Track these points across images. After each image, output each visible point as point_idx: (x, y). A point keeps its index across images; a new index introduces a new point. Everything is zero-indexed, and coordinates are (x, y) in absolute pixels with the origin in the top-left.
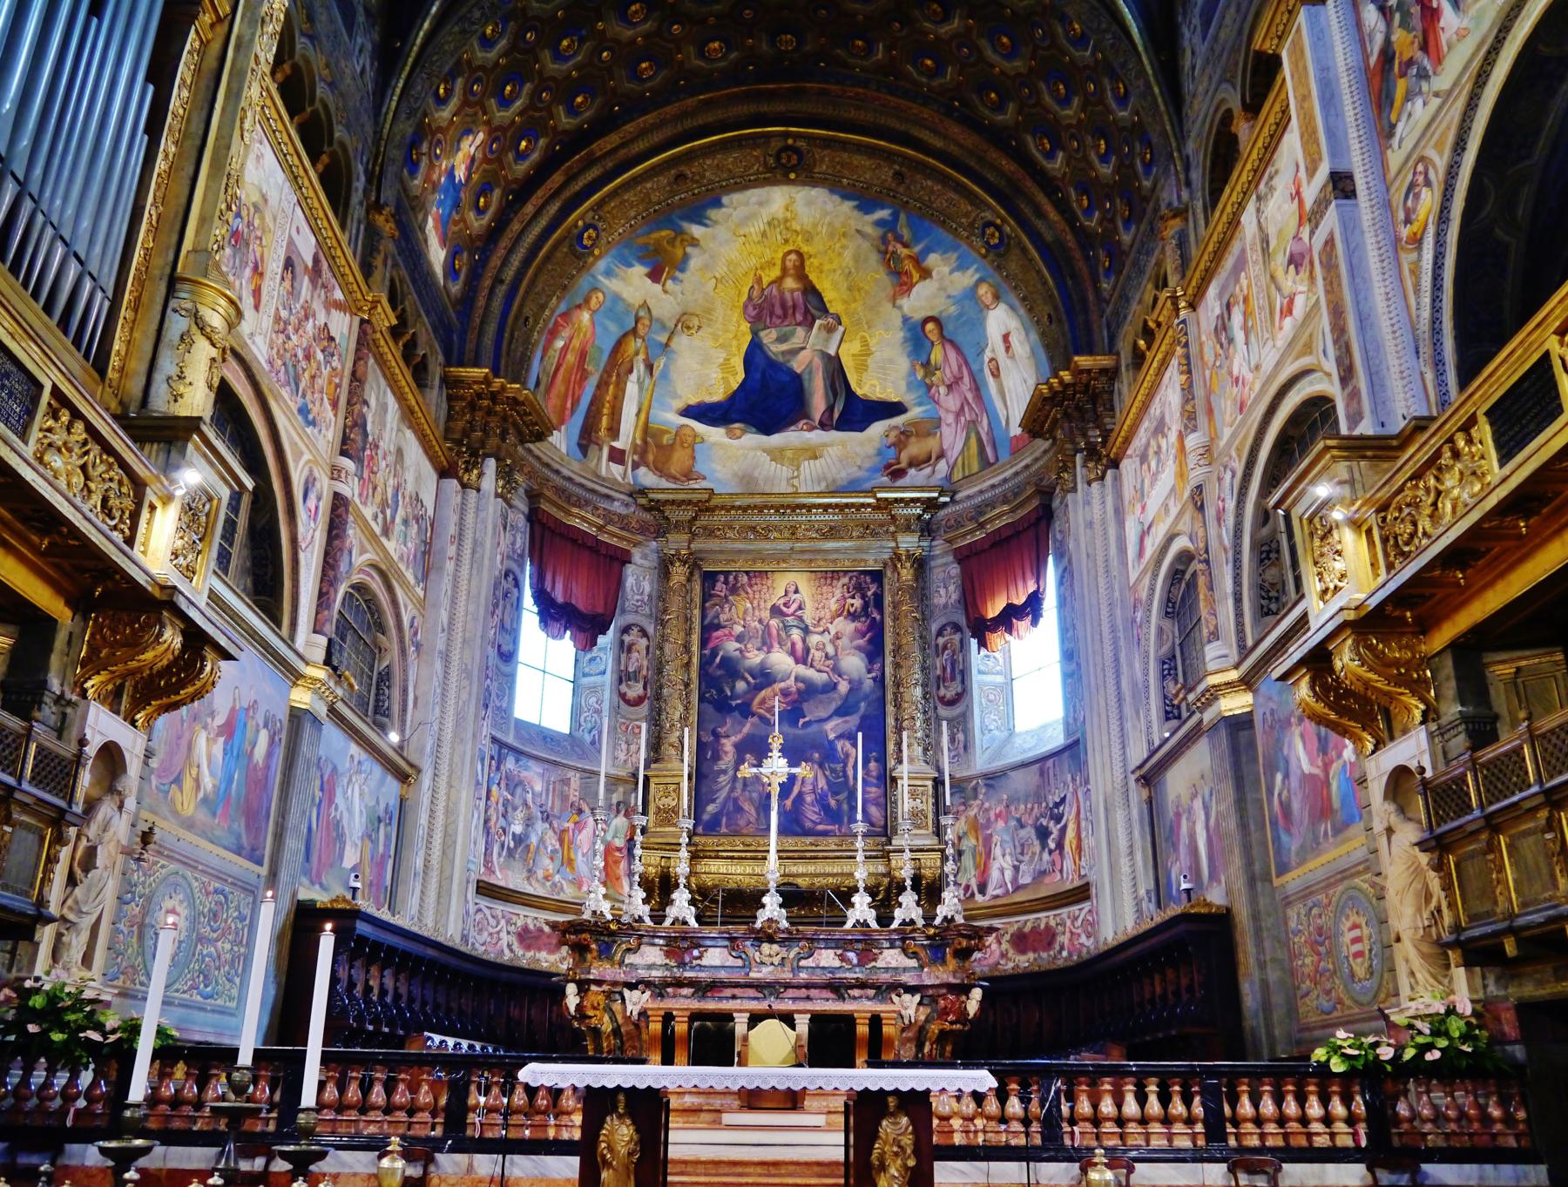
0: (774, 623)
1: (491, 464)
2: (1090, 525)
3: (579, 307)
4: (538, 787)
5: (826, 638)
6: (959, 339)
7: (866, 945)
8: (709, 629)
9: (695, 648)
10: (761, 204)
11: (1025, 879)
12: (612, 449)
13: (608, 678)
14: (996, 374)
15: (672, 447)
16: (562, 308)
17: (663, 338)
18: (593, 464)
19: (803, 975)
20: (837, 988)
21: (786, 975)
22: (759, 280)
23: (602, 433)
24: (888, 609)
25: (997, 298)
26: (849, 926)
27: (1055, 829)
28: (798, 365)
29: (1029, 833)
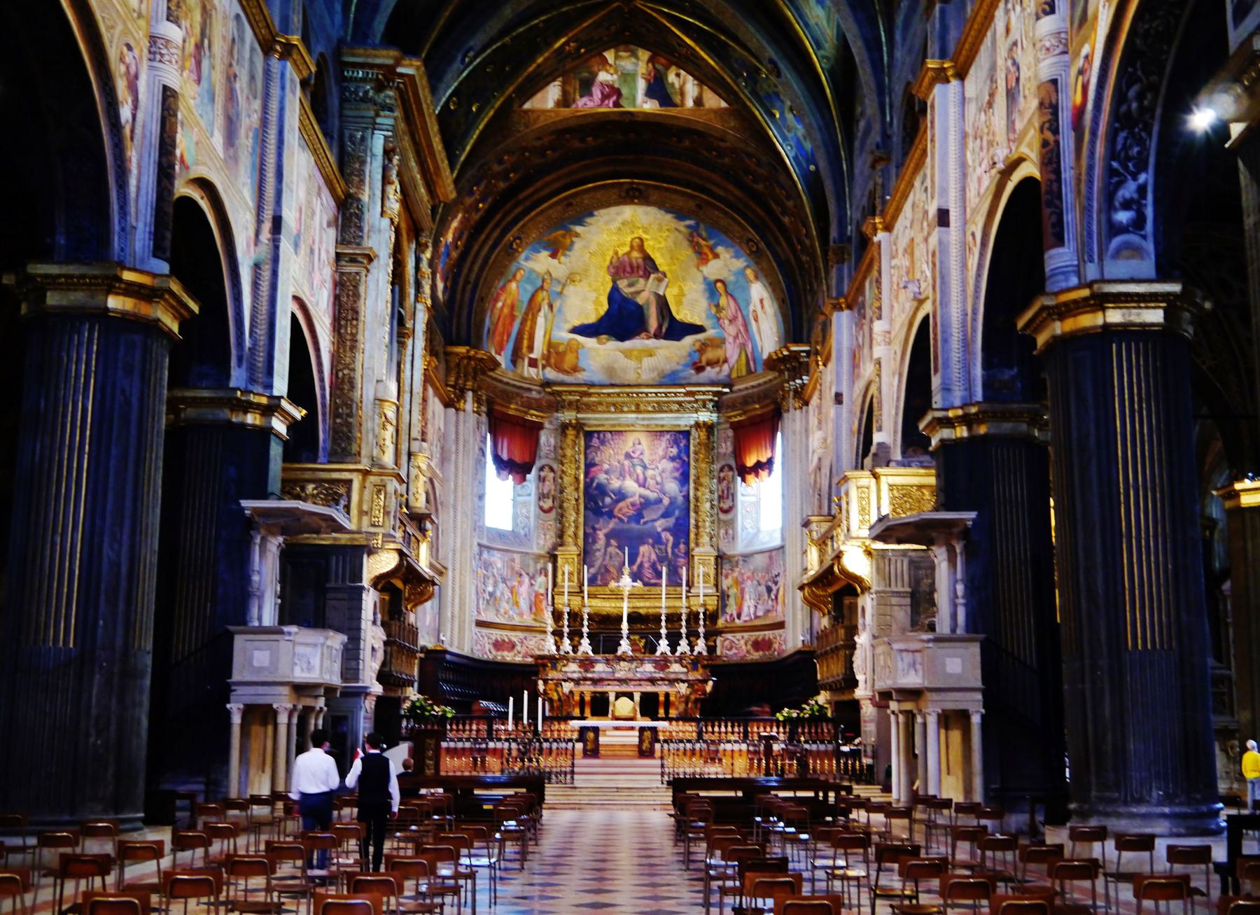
0: (627, 463)
1: (470, 394)
2: (794, 433)
3: (510, 281)
4: (499, 565)
5: (656, 472)
6: (736, 295)
7: (663, 664)
8: (589, 466)
9: (582, 477)
10: (618, 214)
11: (760, 613)
12: (530, 359)
13: (533, 498)
14: (756, 320)
15: (564, 353)
16: (501, 284)
17: (559, 289)
18: (519, 371)
19: (638, 675)
20: (652, 681)
21: (630, 676)
22: (616, 253)
23: (525, 350)
24: (692, 455)
25: (757, 278)
26: (658, 654)
27: (774, 588)
28: (640, 300)
29: (763, 589)
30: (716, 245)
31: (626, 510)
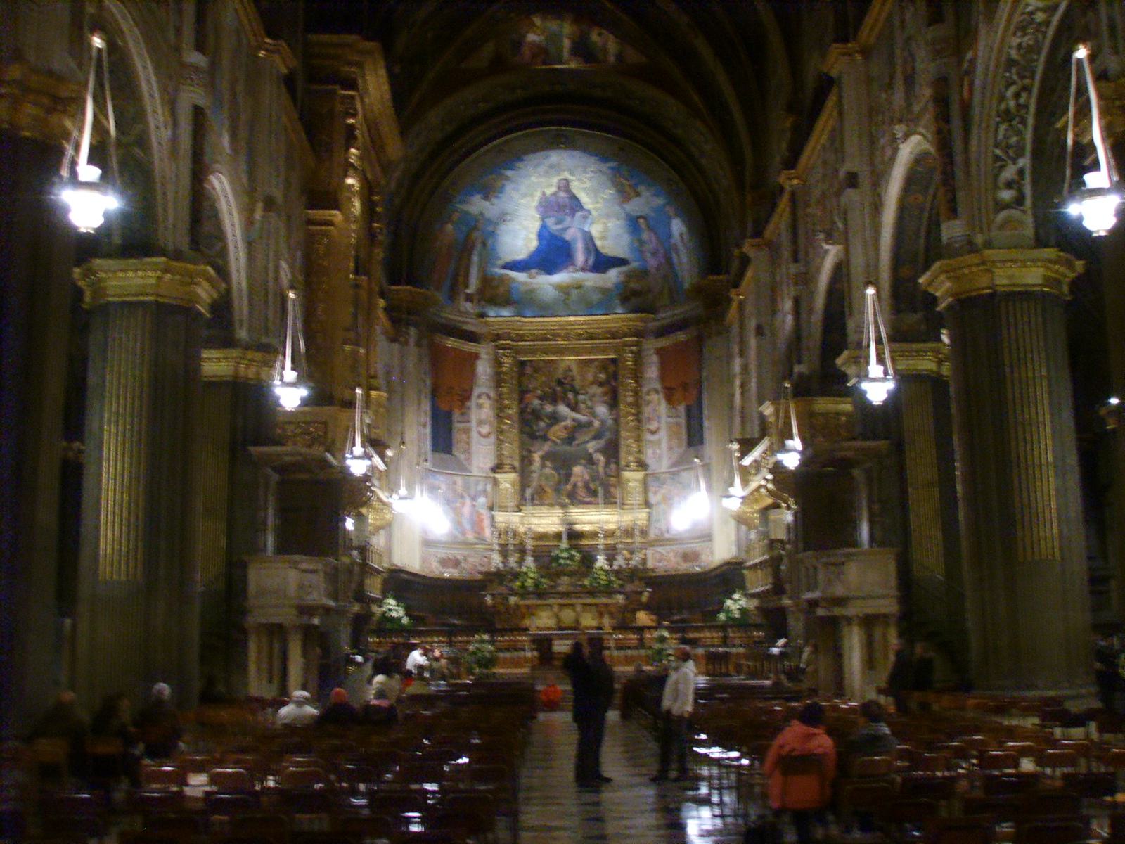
0: (559, 389)
22: (544, 194)
30: (636, 185)
31: (559, 433)
